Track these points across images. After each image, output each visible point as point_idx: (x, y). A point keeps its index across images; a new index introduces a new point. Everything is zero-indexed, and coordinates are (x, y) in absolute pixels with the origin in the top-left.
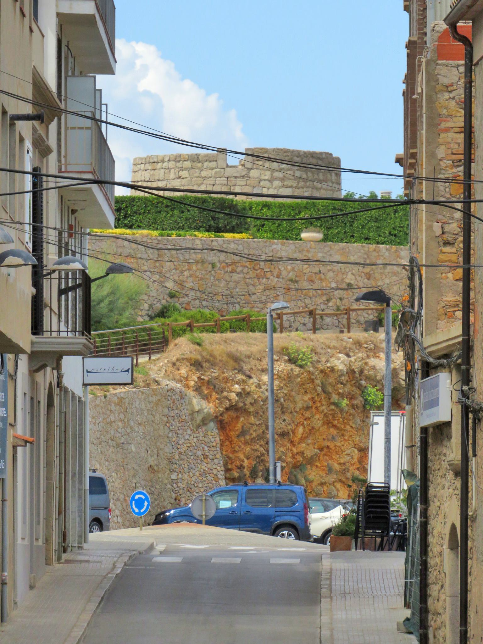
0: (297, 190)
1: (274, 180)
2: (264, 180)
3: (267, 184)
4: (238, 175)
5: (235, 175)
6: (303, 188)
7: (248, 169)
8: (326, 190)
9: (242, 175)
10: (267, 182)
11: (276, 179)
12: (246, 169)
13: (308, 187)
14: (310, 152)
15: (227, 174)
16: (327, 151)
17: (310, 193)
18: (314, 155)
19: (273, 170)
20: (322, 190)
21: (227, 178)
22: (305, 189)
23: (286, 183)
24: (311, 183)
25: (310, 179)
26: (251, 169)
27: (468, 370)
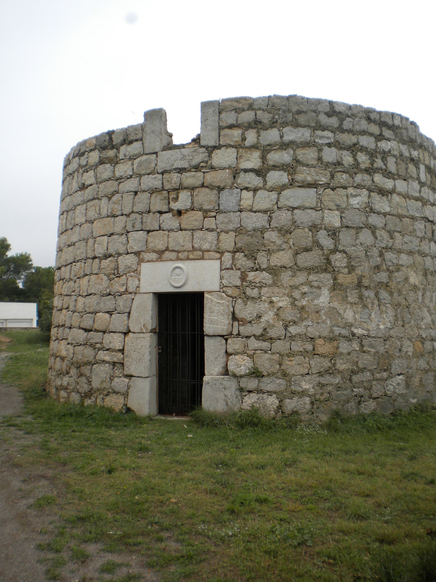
0: (328, 191)
1: (269, 170)
2: (246, 171)
3: (254, 180)
4: (186, 165)
5: (179, 164)
6: (345, 188)
7: (207, 147)
8: (406, 196)
9: (195, 162)
10: (252, 176)
11: (275, 167)
12: (203, 150)
13: (358, 187)
14: (361, 107)
15: (162, 166)
16: (404, 114)
17: (366, 200)
18: (372, 116)
19: (265, 150)
20: (395, 195)
21: (162, 173)
22: (351, 190)
23: (299, 177)
24: (367, 177)
25: (363, 166)
26: (215, 148)
27: (211, 147)
